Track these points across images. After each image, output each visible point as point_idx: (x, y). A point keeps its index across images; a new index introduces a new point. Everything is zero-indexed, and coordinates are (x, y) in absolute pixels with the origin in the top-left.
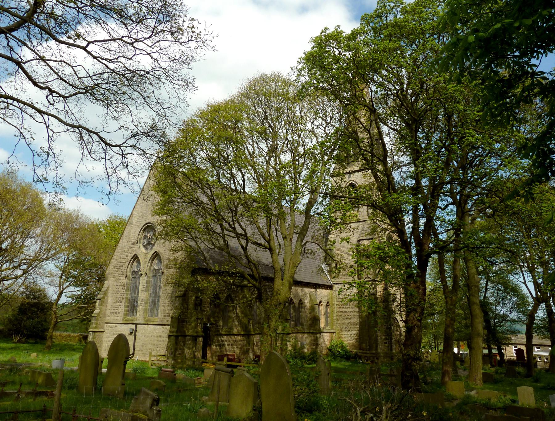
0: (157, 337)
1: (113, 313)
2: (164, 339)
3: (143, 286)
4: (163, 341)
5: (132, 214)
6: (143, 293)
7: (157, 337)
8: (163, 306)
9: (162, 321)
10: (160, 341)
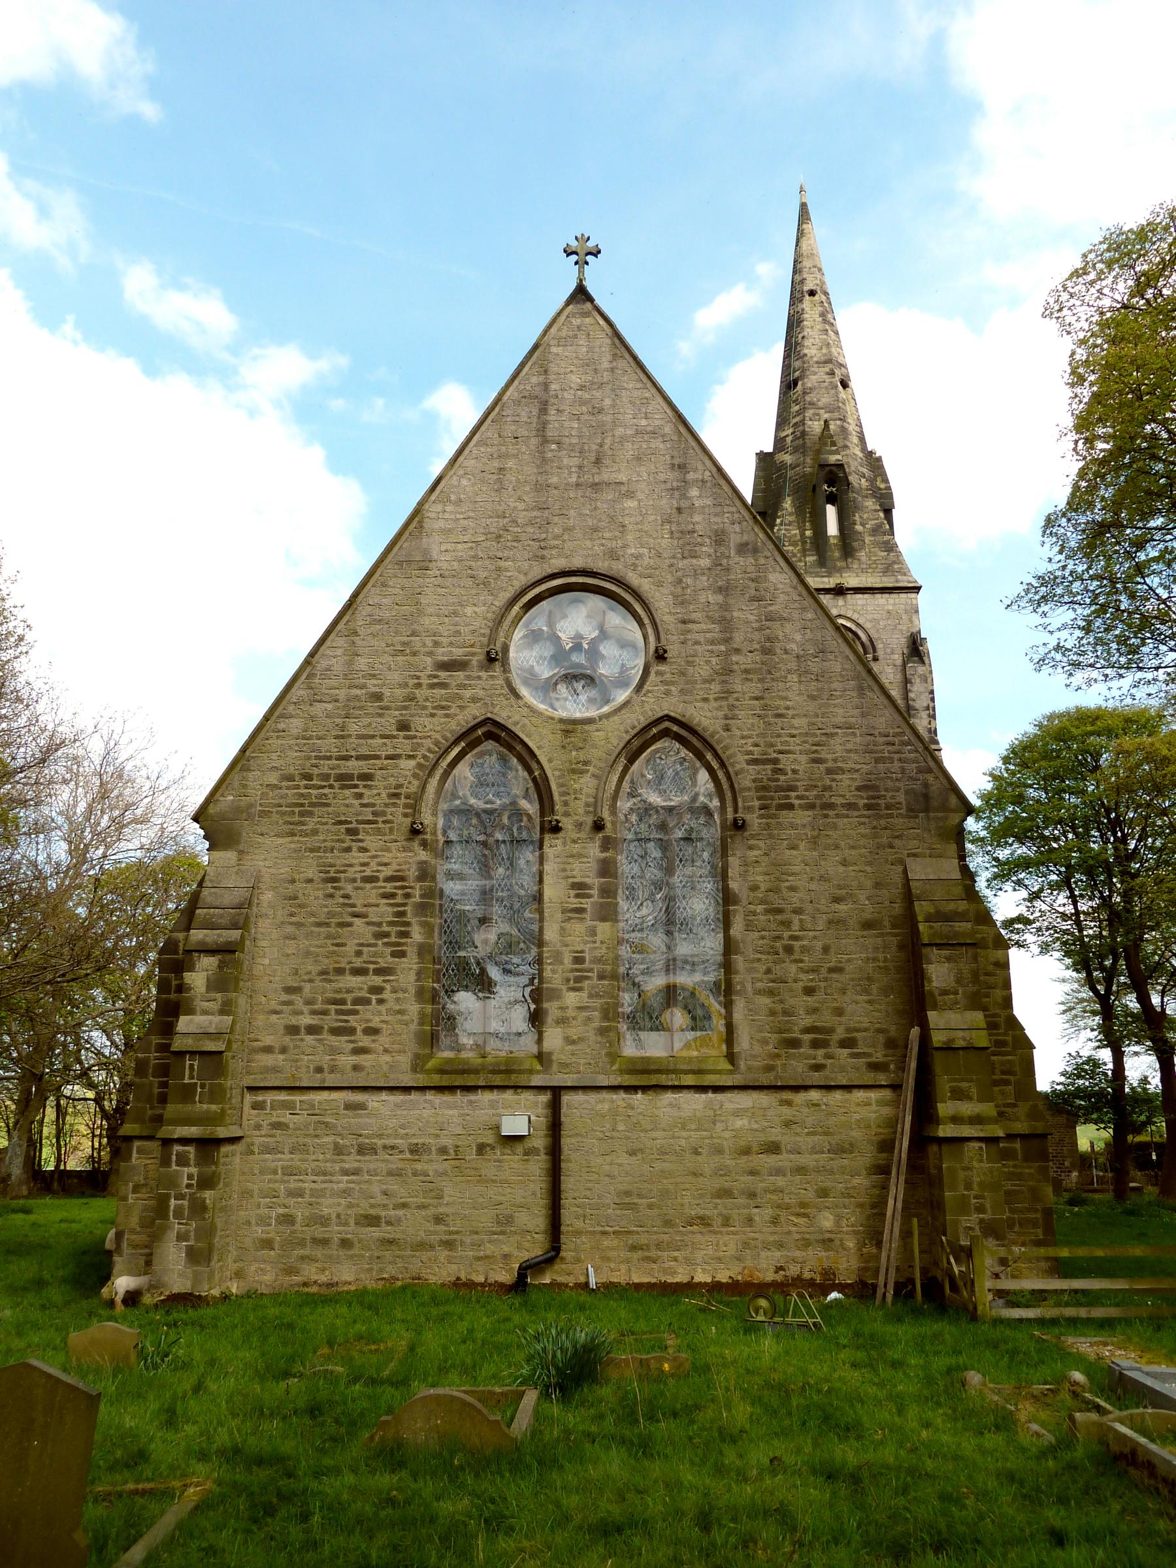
0: (746, 1151)
1: (312, 1030)
2: (806, 1160)
3: (580, 888)
4: (801, 1170)
5: (417, 512)
6: (578, 928)
7: (746, 1151)
8: (771, 993)
9: (770, 1068)
10: (779, 1172)
